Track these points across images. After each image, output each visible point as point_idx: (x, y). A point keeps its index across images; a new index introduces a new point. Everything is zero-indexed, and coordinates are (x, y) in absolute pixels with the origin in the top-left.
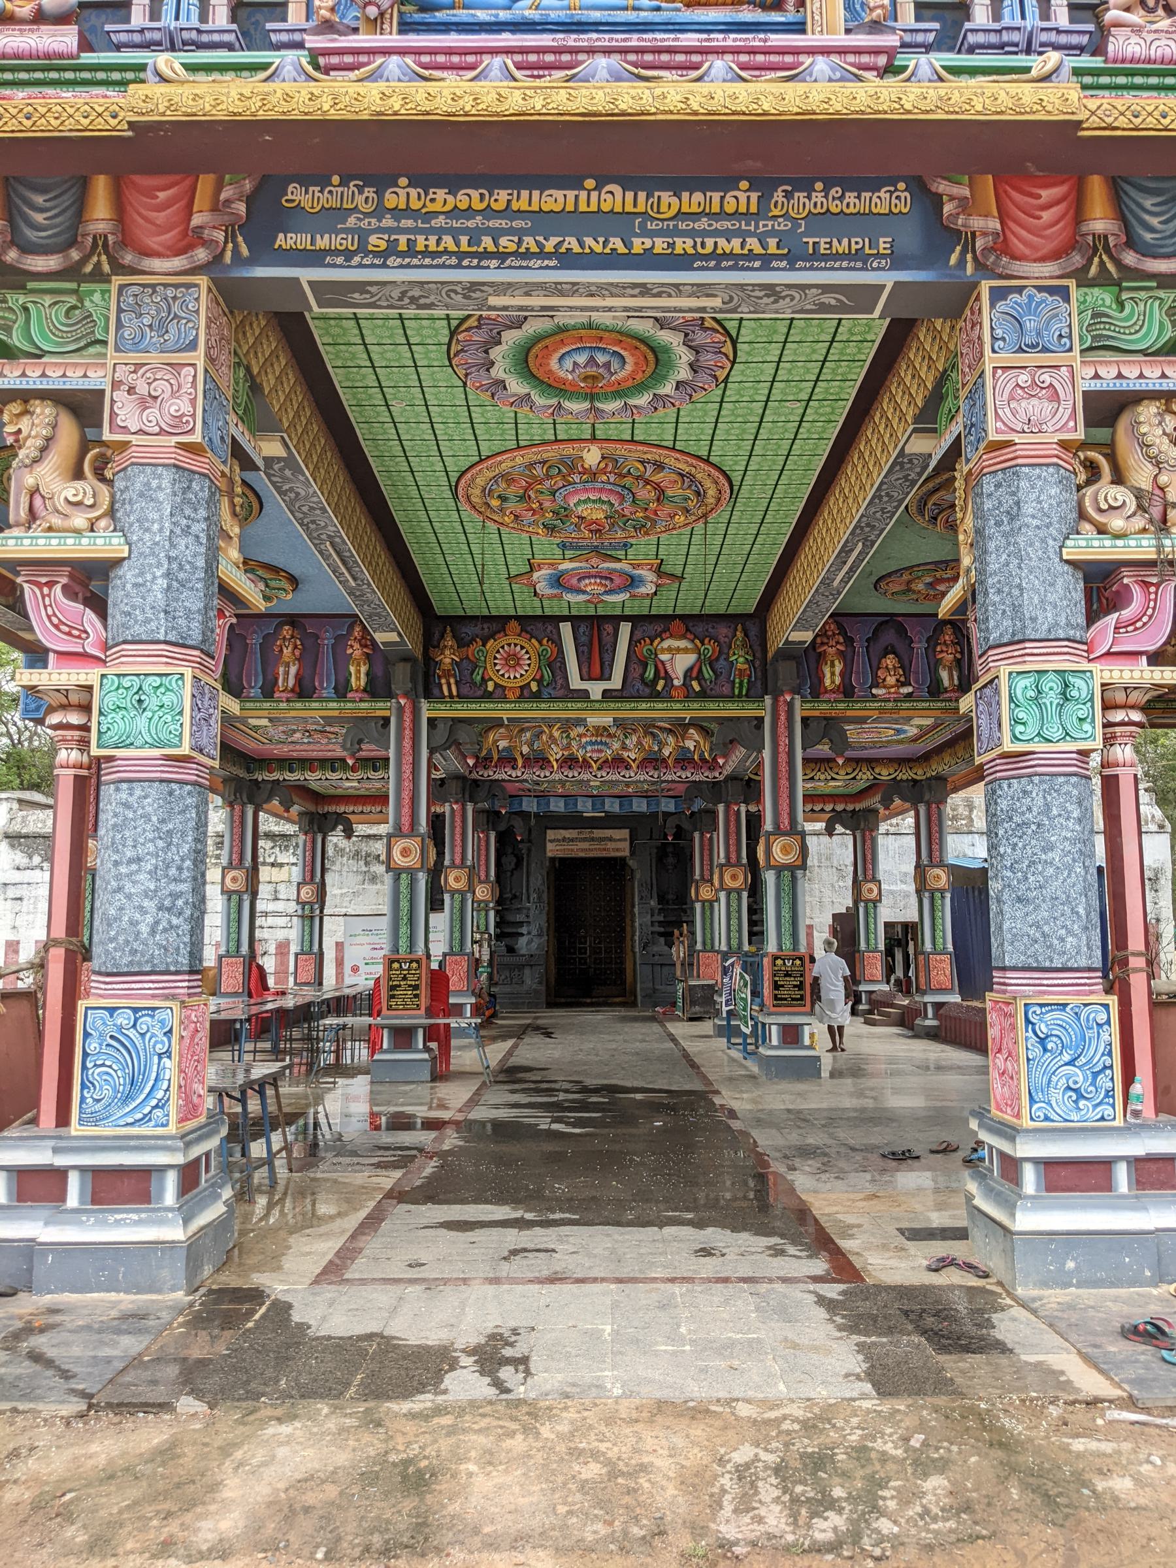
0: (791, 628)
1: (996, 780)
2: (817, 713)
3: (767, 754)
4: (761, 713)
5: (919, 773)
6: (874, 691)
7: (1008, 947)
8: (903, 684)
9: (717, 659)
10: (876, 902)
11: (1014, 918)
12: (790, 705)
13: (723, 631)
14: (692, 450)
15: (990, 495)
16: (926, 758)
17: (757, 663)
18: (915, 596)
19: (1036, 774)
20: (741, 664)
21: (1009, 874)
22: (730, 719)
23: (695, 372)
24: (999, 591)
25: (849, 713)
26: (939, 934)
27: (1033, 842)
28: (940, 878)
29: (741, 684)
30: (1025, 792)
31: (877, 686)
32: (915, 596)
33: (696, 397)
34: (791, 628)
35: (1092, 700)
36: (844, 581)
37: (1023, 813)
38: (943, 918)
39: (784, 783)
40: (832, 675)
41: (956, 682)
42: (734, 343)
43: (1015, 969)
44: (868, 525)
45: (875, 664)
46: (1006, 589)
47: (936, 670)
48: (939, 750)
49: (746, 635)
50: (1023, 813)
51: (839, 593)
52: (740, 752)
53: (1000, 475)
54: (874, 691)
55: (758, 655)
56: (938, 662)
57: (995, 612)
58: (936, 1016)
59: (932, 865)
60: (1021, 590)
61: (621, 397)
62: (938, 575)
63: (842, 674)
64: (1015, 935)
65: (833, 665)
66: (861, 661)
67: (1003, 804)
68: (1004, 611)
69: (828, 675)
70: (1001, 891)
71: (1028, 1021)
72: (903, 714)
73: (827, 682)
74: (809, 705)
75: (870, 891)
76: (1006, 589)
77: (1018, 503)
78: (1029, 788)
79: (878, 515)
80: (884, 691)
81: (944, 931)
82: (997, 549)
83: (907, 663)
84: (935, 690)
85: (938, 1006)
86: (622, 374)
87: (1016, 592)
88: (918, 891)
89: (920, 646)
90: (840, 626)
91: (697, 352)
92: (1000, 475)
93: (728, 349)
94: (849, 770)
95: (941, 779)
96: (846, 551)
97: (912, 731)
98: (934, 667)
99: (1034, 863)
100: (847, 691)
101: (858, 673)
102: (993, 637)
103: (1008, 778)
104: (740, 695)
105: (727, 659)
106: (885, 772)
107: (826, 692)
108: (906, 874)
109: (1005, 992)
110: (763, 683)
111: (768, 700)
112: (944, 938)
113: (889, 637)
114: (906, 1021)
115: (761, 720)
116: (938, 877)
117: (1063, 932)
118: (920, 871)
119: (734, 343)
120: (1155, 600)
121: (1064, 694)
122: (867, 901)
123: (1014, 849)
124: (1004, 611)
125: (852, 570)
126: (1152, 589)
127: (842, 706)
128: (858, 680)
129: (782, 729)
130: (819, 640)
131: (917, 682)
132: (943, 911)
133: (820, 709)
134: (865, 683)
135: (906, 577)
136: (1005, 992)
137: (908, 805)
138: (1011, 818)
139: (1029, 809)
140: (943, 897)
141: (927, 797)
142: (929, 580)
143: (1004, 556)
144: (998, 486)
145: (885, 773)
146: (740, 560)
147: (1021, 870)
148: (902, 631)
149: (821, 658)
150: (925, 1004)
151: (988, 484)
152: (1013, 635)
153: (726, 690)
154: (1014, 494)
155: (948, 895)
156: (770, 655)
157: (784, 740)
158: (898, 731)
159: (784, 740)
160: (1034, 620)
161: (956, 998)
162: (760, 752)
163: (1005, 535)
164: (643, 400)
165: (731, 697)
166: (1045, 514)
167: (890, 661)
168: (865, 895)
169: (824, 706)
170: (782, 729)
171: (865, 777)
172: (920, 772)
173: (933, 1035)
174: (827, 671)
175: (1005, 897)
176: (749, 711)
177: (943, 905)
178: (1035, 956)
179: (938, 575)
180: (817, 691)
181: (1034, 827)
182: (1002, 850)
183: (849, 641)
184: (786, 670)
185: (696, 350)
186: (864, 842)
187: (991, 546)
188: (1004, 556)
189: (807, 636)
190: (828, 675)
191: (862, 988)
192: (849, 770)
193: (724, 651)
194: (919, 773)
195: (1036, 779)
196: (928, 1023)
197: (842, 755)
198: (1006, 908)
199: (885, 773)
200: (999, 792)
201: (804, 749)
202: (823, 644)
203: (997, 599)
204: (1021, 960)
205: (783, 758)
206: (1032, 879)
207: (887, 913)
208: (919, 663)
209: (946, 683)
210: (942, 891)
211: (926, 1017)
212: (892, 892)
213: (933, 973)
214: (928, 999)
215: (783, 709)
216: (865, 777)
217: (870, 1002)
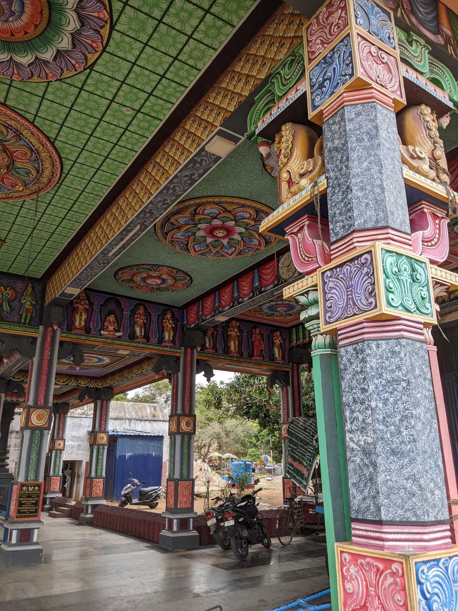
0: (67, 286)
1: (363, 341)
2: (69, 340)
3: (36, 359)
4: (37, 335)
5: (99, 385)
6: (102, 332)
7: (382, 500)
8: (117, 331)
9: (13, 300)
10: (61, 450)
11: (388, 471)
12: (54, 332)
13: (19, 285)
14: (45, 129)
15: (351, 120)
16: (105, 377)
17: (38, 307)
18: (132, 285)
19: (403, 338)
20: (28, 305)
21: (381, 427)
22: (16, 336)
23: (74, 46)
24: (362, 189)
25: (87, 342)
26: (99, 467)
27: (405, 398)
28: (103, 439)
29: (26, 316)
30: (393, 352)
31: (103, 330)
32: (132, 285)
33: (67, 74)
34: (67, 286)
35: (427, 285)
36: (115, 255)
37: (393, 371)
38: (102, 459)
39: (44, 377)
40: (80, 320)
41: (143, 334)
42: (112, 28)
43: (392, 523)
44: (150, 211)
45: (103, 318)
46: (369, 188)
47: (134, 327)
48: (113, 374)
49: (33, 290)
50: (393, 371)
51: (108, 263)
52: (18, 356)
53: (360, 108)
54: (102, 332)
55: (39, 302)
56: (135, 323)
57: (359, 204)
58: (92, 512)
59: (101, 432)
60: (383, 189)
61: (9, 51)
62: (150, 273)
63: (86, 321)
64: (391, 488)
65: (81, 315)
66: (96, 316)
67: (373, 362)
68: (367, 204)
69: (78, 320)
70: (374, 444)
71: (419, 583)
72: (115, 347)
73: (77, 324)
74: (65, 335)
75: (60, 444)
76: (369, 188)
77: (376, 127)
78: (397, 349)
79: (160, 204)
80: (107, 333)
81: (102, 466)
82: (359, 158)
83: (119, 320)
84: (132, 337)
85: (94, 506)
86: (16, 24)
87: (378, 190)
88: (91, 446)
89: (127, 313)
90: (87, 295)
91: (83, 25)
92: (360, 108)
93: (105, 32)
94: (65, 380)
95: (110, 388)
96: (127, 230)
97: (107, 360)
98: (133, 324)
99: (406, 417)
100: (87, 330)
101: (93, 322)
102: (358, 223)
103: (376, 339)
104: (24, 323)
105: (19, 301)
106: (83, 383)
107: (76, 328)
108: (74, 437)
109: (382, 548)
110: (40, 317)
111: (41, 328)
112: (102, 470)
113: (112, 306)
114: (76, 515)
115: (35, 339)
116: (103, 438)
117: (432, 485)
118: (93, 434)
119: (112, 28)
120: (439, 229)
121: (412, 276)
122: (57, 450)
123: (385, 404)
124: (367, 204)
125: (123, 247)
126: (437, 221)
127: (83, 338)
128: (93, 325)
129: (47, 346)
130: (75, 301)
131: (123, 331)
132: (103, 456)
133: (71, 337)
134: (97, 327)
135: (135, 270)
136: (382, 548)
137: (92, 400)
138: (381, 376)
139: (399, 368)
140: (104, 448)
141: (102, 397)
142: (144, 275)
143: (366, 164)
144: (358, 114)
145: (83, 383)
146: (46, 236)
147: (393, 424)
148: (119, 304)
149: (75, 310)
150: (87, 506)
151: (349, 113)
152: (377, 222)
153: (16, 319)
154: (372, 121)
155: (106, 447)
156: (47, 302)
157: (47, 353)
158: (100, 360)
159: (47, 353)
160: (392, 213)
161: (104, 502)
162: (31, 358)
163: (365, 148)
164: (25, 59)
165: (19, 323)
166: (391, 142)
167: (112, 318)
168: (57, 446)
169: (74, 336)
170: (47, 346)
171: (73, 384)
172: (100, 384)
173: (90, 523)
174: (78, 317)
175: (379, 449)
176: (29, 333)
177: (103, 453)
178: (413, 509)
179: (150, 273)
180: (70, 328)
181: (404, 384)
182: (373, 404)
183: (91, 304)
184: (57, 312)
185: (82, 19)
186: (60, 419)
187: (354, 155)
188: (366, 164)
189: (76, 291)
190: (78, 320)
191: (48, 496)
192: (65, 380)
193: (18, 296)
194: (99, 385)
195: (403, 342)
196: (88, 516)
197: (78, 365)
198: (380, 460)
199: (83, 383)
200: (368, 351)
201: (59, 359)
202: (77, 303)
203: (360, 194)
204: (398, 515)
205: (46, 363)
206: (405, 433)
207: (66, 456)
208: (126, 322)
209: (138, 334)
210: (103, 445)
211: (87, 513)
212: (68, 445)
213: (94, 489)
214: (90, 503)
215: (49, 334)
216: (73, 384)
217: (51, 503)
